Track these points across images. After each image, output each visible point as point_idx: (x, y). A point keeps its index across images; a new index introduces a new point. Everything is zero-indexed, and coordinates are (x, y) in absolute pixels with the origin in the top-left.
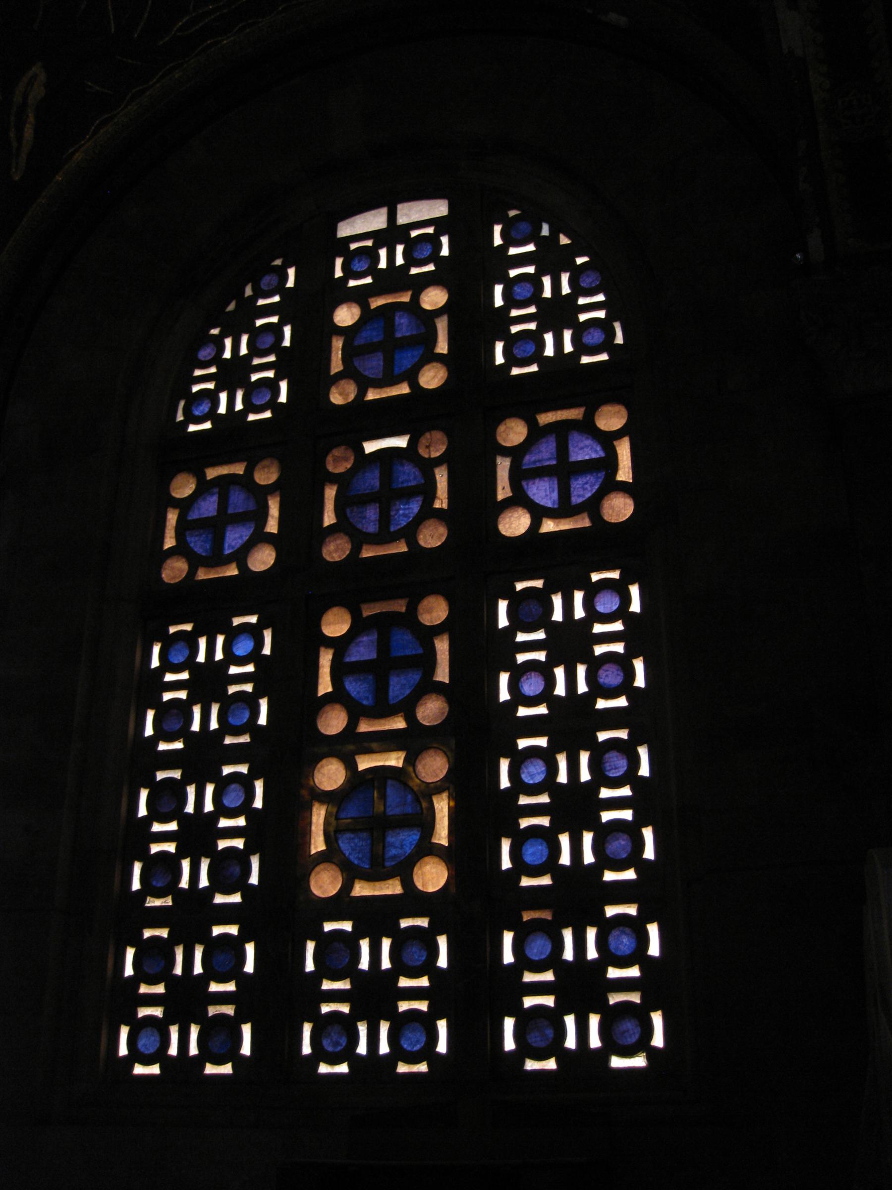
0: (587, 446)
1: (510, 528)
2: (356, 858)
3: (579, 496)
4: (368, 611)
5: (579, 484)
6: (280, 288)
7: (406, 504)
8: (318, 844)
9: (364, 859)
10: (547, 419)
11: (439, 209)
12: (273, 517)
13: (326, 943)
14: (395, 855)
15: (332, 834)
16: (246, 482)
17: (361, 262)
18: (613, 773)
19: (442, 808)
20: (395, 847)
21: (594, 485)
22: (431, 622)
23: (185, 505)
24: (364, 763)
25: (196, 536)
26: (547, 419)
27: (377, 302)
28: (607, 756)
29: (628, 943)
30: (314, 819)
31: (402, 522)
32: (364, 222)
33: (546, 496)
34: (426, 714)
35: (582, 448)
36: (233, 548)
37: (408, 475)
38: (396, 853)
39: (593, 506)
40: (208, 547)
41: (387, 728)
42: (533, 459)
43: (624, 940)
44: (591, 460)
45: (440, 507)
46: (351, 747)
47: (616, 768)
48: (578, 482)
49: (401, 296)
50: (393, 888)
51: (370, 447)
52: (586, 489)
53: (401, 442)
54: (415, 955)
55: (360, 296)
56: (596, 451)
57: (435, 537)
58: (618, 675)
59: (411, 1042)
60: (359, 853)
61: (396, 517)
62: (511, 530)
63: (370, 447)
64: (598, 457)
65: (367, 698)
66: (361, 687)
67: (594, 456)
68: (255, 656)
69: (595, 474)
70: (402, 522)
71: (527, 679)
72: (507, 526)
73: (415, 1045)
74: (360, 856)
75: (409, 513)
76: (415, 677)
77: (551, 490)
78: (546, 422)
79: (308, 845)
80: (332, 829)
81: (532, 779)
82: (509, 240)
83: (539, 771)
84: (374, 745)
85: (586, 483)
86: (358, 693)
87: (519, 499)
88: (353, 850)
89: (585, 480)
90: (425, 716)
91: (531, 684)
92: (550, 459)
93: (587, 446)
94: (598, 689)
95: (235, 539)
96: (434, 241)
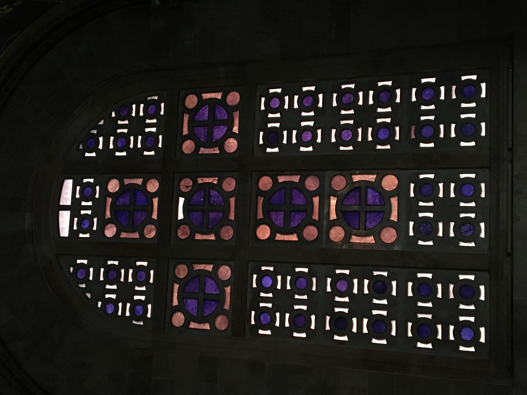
0: (203, 112)
1: (233, 147)
2: (379, 219)
3: (225, 116)
4: (260, 216)
5: (219, 115)
6: (85, 268)
7: (212, 197)
8: (370, 240)
9: (380, 215)
10: (186, 130)
11: (69, 184)
12: (205, 267)
13: (419, 235)
14: (379, 200)
15: (366, 231)
16: (185, 284)
17: (85, 223)
18: (352, 99)
19: (359, 177)
20: (375, 200)
21: (221, 109)
22: (271, 184)
23: (189, 319)
24: (333, 216)
25: (206, 310)
26: (186, 130)
27: (108, 214)
28: (344, 102)
29: (429, 91)
30: (358, 241)
31: (221, 199)
32: (64, 223)
33: (222, 130)
34: (314, 186)
35: (203, 115)
36: (216, 289)
37: (198, 197)
38: (378, 199)
39: (230, 109)
40: (214, 303)
41: (318, 205)
42: (203, 137)
43: (428, 93)
44: (209, 110)
45: (217, 180)
46: (325, 223)
47: (350, 98)
48: (218, 116)
49: (108, 202)
50: (394, 201)
51: (181, 216)
52: (222, 112)
53: (182, 200)
54: (428, 189)
55: (102, 226)
56: (206, 108)
57: (231, 183)
58: (308, 98)
59: (471, 190)
60: (376, 218)
61: (218, 202)
62: (235, 146)
63: (181, 216)
64: (208, 107)
65: (302, 215)
66: (297, 218)
67: (207, 109)
68: (273, 275)
69: (216, 109)
70: (221, 199)
71: (304, 138)
72: (232, 148)
73: (472, 189)
74: (378, 217)
75: (217, 196)
76: (295, 193)
77: (219, 128)
78: (187, 130)
79: (371, 244)
80: (364, 232)
81: (350, 135)
82: (95, 149)
83: (347, 132)
84: (326, 210)
85: (219, 112)
86: (299, 219)
87: (221, 144)
88: (374, 221)
89: (218, 113)
90: (315, 186)
91: (307, 136)
92: (205, 129)
93: (203, 112)
94: (314, 107)
95: (212, 288)
96: (84, 187)
